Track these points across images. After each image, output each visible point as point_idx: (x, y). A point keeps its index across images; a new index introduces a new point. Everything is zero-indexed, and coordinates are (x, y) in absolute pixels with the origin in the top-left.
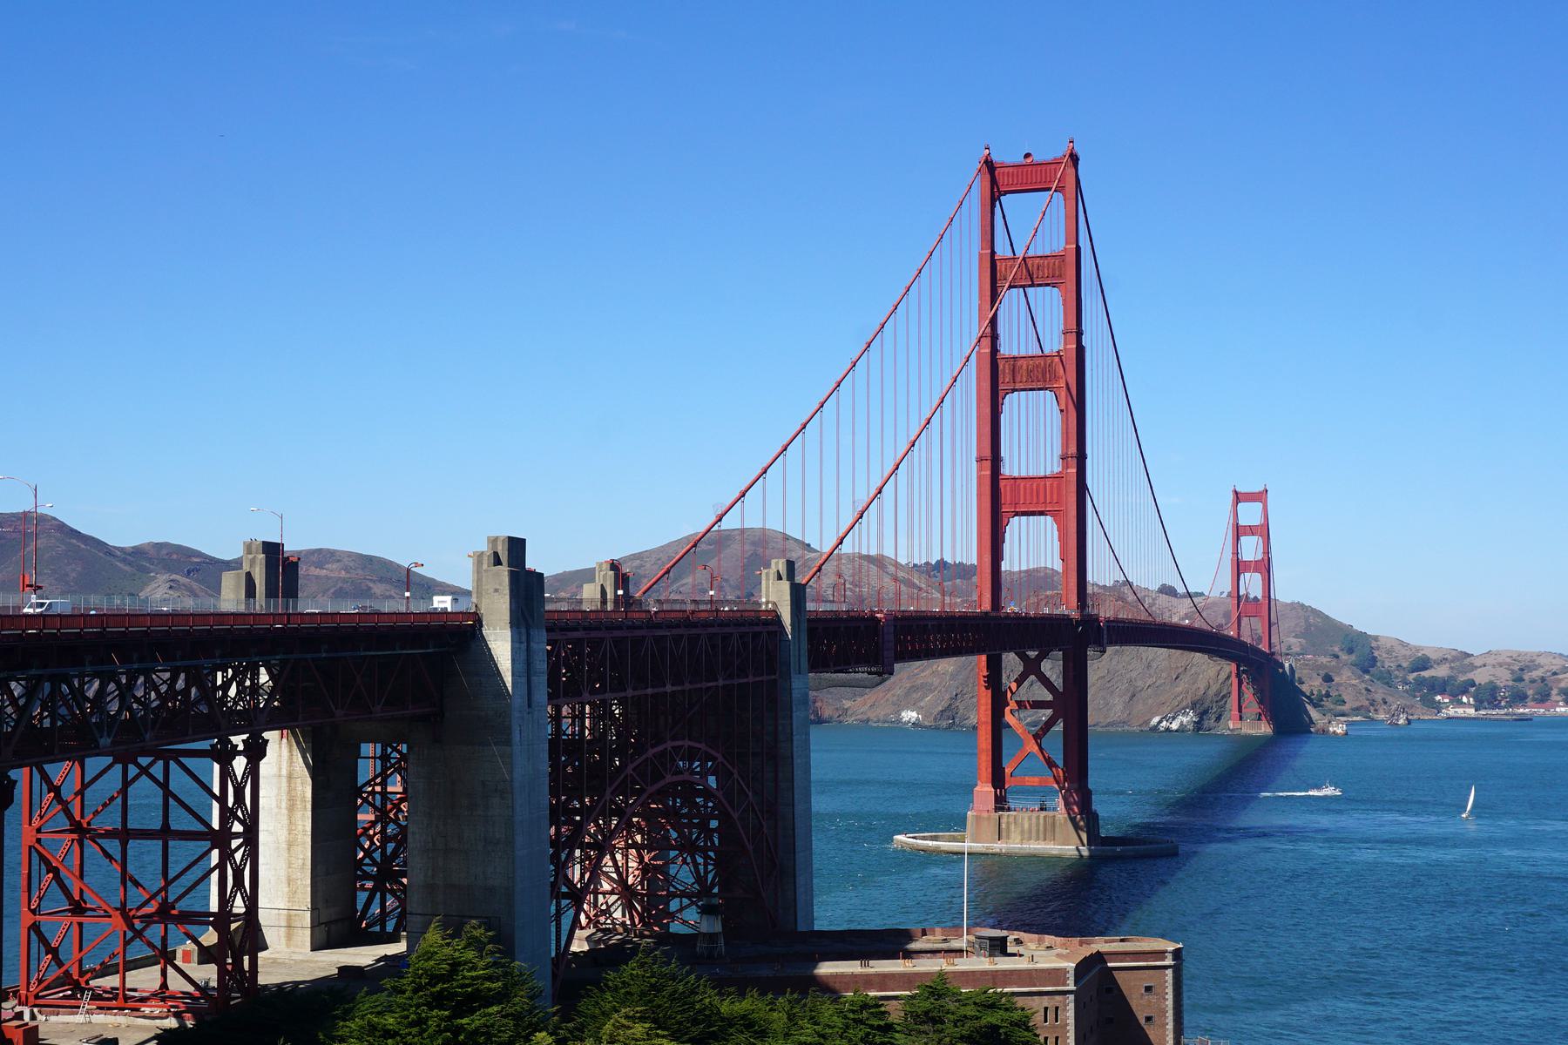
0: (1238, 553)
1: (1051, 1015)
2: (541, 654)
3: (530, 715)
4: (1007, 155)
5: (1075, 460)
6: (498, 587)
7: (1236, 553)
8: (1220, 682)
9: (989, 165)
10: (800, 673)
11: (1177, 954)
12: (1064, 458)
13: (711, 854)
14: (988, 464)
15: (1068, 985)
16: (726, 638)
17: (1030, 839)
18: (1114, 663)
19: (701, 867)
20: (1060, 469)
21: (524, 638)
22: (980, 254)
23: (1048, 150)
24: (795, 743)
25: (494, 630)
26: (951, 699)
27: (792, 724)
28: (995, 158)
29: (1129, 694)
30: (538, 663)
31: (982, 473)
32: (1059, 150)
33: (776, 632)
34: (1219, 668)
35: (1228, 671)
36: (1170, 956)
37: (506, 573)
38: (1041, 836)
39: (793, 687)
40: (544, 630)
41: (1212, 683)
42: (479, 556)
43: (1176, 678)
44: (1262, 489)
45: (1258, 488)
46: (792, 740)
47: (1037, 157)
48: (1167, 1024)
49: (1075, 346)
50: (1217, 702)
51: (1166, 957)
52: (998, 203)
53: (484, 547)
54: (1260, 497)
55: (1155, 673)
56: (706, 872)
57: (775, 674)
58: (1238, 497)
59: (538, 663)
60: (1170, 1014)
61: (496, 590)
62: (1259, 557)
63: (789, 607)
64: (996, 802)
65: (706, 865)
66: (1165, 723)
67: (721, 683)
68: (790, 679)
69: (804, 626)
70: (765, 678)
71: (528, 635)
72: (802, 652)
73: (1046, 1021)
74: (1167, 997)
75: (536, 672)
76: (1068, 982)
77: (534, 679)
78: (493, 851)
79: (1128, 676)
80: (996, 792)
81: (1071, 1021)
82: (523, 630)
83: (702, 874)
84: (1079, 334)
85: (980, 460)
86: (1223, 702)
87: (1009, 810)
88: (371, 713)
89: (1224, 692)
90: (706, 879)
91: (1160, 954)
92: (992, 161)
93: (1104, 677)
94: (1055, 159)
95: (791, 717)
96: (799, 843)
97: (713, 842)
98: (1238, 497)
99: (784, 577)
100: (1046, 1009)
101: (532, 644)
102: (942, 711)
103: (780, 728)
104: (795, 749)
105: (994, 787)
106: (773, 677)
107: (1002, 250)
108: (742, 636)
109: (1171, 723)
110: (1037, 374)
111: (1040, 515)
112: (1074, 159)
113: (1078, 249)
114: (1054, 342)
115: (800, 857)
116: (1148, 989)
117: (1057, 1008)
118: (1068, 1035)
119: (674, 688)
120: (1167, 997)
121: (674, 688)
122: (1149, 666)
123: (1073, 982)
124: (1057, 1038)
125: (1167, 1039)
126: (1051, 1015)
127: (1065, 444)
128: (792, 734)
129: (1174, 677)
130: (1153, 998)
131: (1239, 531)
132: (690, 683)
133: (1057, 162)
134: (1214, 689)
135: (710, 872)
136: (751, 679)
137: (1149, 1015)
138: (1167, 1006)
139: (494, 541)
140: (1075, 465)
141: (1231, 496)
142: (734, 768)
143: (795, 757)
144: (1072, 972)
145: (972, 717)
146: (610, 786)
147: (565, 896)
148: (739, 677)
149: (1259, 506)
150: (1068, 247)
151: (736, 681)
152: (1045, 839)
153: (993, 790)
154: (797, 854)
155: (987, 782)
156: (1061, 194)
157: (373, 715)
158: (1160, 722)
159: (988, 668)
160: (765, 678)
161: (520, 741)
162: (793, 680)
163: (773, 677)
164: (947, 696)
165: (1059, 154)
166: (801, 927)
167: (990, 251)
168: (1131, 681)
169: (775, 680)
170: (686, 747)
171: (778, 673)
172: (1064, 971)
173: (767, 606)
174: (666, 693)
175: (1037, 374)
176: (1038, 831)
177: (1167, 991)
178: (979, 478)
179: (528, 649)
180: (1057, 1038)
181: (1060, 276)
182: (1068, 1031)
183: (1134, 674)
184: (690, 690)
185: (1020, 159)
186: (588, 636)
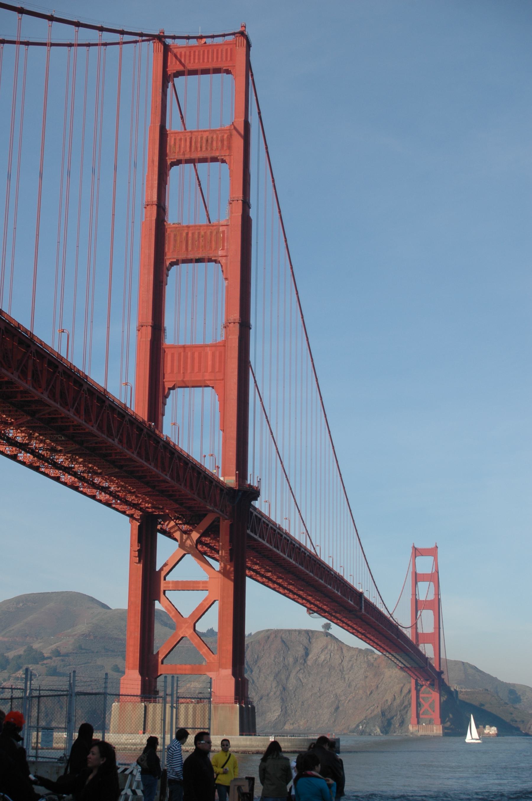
0: (416, 595)
5: (238, 326)
7: (415, 594)
8: (403, 694)
34: (402, 685)
35: (408, 687)
41: (397, 697)
43: (371, 693)
44: (433, 546)
45: (431, 546)
52: (170, 84)
54: (433, 552)
55: (355, 689)
58: (417, 552)
66: (361, 727)
79: (334, 693)
85: (140, 327)
86: (405, 711)
89: (406, 703)
93: (316, 693)
98: (417, 552)
113: (247, 125)
122: (349, 686)
129: (369, 693)
131: (417, 578)
134: (398, 701)
141: (411, 550)
149: (431, 558)
158: (358, 726)
168: (336, 695)
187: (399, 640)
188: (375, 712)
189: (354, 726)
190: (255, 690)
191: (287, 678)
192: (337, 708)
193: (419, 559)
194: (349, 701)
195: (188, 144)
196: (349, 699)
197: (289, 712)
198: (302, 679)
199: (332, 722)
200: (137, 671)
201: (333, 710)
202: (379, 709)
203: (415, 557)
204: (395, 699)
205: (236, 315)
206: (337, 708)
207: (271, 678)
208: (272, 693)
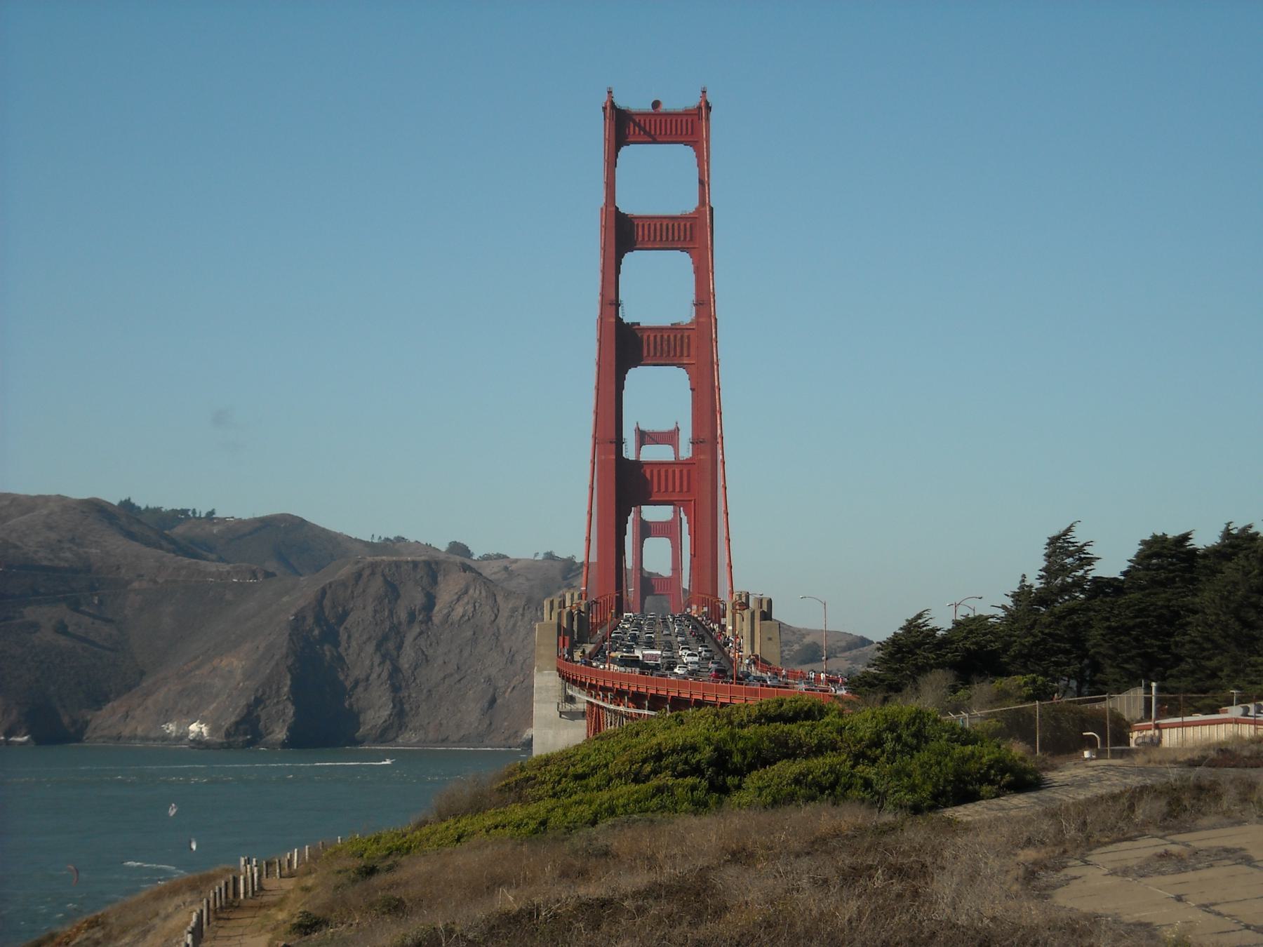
4: (635, 101)
6: (771, 636)
18: (466, 654)
23: (678, 101)
26: (249, 706)
32: (692, 102)
47: (666, 106)
55: (522, 668)
61: (770, 639)
93: (452, 675)
94: (686, 110)
102: (237, 724)
122: (512, 661)
145: (277, 730)
164: (243, 702)
168: (490, 679)
185: (647, 107)
190: (343, 669)
191: (400, 647)
192: (493, 701)
194: (514, 688)
195: (646, 232)
196: (512, 686)
197: (407, 707)
198: (424, 650)
199: (485, 726)
201: (486, 705)
203: (641, 447)
206: (493, 701)
207: (370, 648)
208: (374, 676)
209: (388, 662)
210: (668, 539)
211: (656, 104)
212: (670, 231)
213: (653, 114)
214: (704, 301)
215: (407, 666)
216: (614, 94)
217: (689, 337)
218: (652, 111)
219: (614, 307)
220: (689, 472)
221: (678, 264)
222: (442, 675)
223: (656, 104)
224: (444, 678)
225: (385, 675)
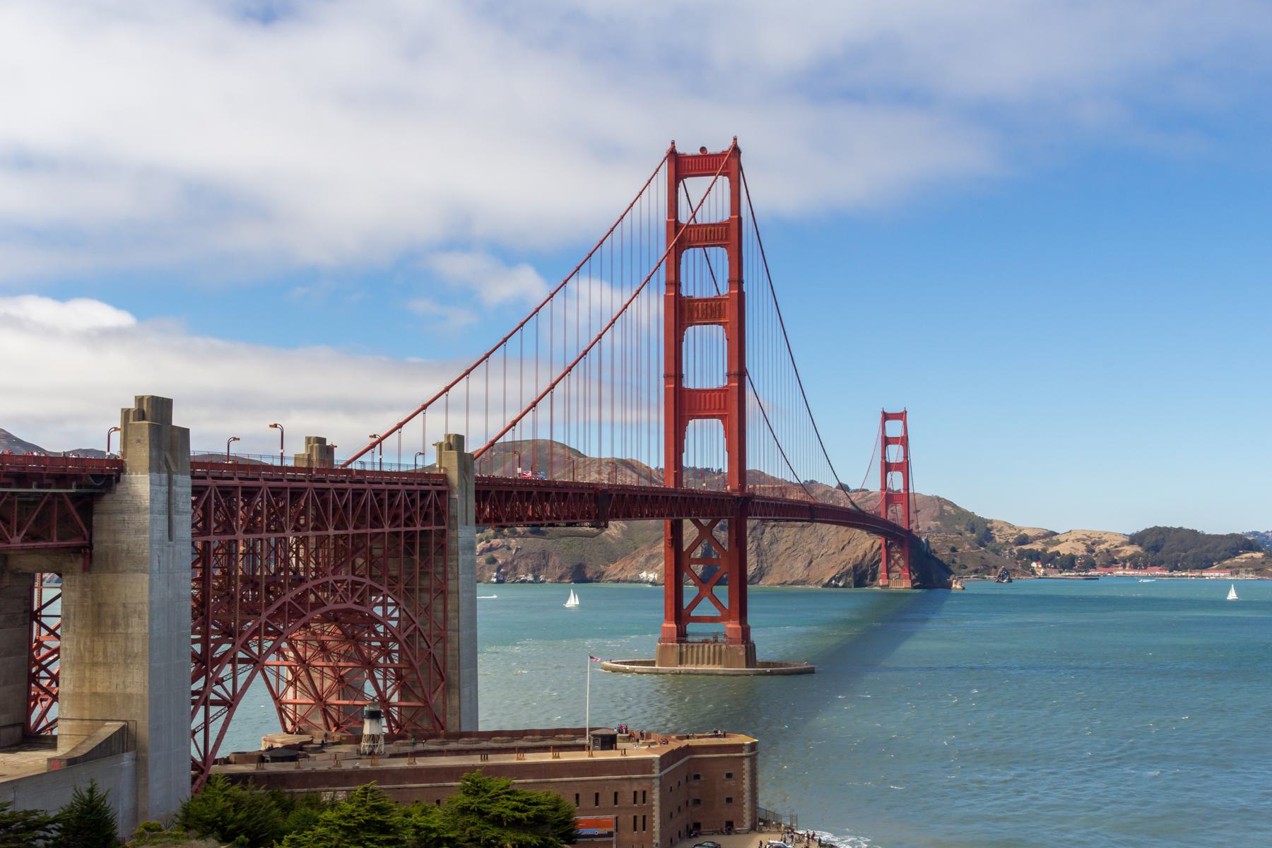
1: (640, 798)
2: (185, 496)
3: (172, 548)
4: (688, 148)
6: (139, 438)
7: (884, 457)
8: (874, 550)
9: (674, 156)
10: (467, 525)
11: (753, 746)
12: (729, 375)
13: (392, 670)
14: (672, 380)
15: (654, 773)
16: (392, 494)
17: (703, 663)
18: (798, 537)
19: (381, 683)
20: (726, 384)
21: (165, 482)
22: (668, 222)
24: (460, 581)
25: (137, 474)
27: (458, 565)
28: (679, 150)
29: (808, 561)
30: (181, 503)
31: (667, 386)
32: (726, 146)
33: (444, 492)
36: (747, 749)
37: (147, 426)
38: (711, 660)
39: (460, 535)
40: (189, 477)
41: (867, 552)
42: (126, 413)
43: (843, 548)
45: (901, 410)
46: (458, 579)
47: (710, 151)
48: (744, 804)
49: (737, 291)
50: (872, 566)
51: (743, 750)
53: (132, 405)
54: (901, 416)
55: (827, 545)
56: (386, 688)
57: (444, 524)
58: (886, 417)
59: (181, 503)
60: (747, 796)
61: (138, 441)
62: (901, 460)
63: (457, 472)
64: (678, 636)
65: (385, 680)
66: (834, 581)
67: (387, 529)
68: (457, 529)
69: (472, 488)
70: (433, 528)
71: (170, 482)
72: (469, 508)
73: (635, 802)
74: (744, 781)
75: (178, 512)
76: (654, 770)
77: (176, 518)
78: (131, 663)
80: (678, 628)
81: (656, 803)
82: (165, 476)
83: (382, 690)
84: (740, 282)
85: (666, 376)
87: (687, 642)
88: (9, 543)
89: (876, 559)
90: (385, 691)
91: (739, 747)
92: (676, 153)
93: (790, 548)
95: (458, 560)
96: (464, 662)
97: (392, 661)
98: (886, 417)
99: (454, 448)
100: (635, 793)
101: (174, 487)
103: (449, 569)
104: (460, 586)
105: (676, 624)
106: (442, 527)
107: (684, 217)
108: (410, 493)
109: (839, 582)
110: (710, 311)
111: (712, 418)
112: (736, 151)
113: (740, 219)
114: (724, 290)
115: (465, 673)
116: (729, 776)
117: (644, 792)
118: (654, 814)
119: (338, 532)
120: (744, 781)
121: (338, 532)
122: (822, 540)
123: (658, 770)
124: (644, 817)
125: (654, 819)
126: (640, 798)
127: (730, 366)
128: (458, 572)
129: (841, 548)
130: (732, 782)
131: (886, 441)
132: (356, 528)
133: (723, 154)
134: (869, 556)
135: (390, 687)
136: (419, 528)
137: (729, 796)
138: (744, 789)
139: (140, 400)
140: (737, 381)
142: (400, 600)
143: (460, 591)
144: (657, 762)
146: (266, 610)
147: (215, 703)
148: (407, 525)
149: (900, 423)
150: (732, 217)
151: (403, 529)
152: (714, 663)
153: (675, 626)
154: (461, 671)
155: (671, 620)
156: (726, 179)
157: (10, 545)
158: (831, 580)
159: (672, 533)
160: (433, 528)
161: (159, 570)
162: (459, 530)
163: (442, 527)
165: (726, 149)
166: (465, 728)
167: (674, 220)
168: (810, 551)
169: (445, 530)
170: (350, 581)
171: (446, 524)
172: (650, 761)
173: (440, 471)
174: (329, 536)
175: (710, 311)
176: (709, 658)
177: (744, 777)
178: (666, 390)
179: (169, 492)
180: (644, 817)
181: (726, 239)
182: (654, 811)
183: (812, 546)
184: (353, 535)
185: (698, 152)
186: (242, 484)
187: (867, 524)
188: (847, 567)
189: (827, 581)
191: (763, 534)
192: (811, 562)
193: (888, 423)
194: (822, 555)
196: (822, 553)
197: (765, 565)
200: (674, 622)
202: (851, 565)
204: (865, 555)
205: (735, 369)
209: (756, 541)
210: (901, 473)
211: (703, 149)
212: (712, 233)
213: (701, 156)
214: (737, 280)
215: (766, 543)
216: (676, 145)
217: (725, 304)
218: (700, 154)
219: (674, 285)
220: (725, 396)
221: (720, 256)
222: (784, 548)
223: (703, 149)
224: (786, 550)
225: (754, 547)
